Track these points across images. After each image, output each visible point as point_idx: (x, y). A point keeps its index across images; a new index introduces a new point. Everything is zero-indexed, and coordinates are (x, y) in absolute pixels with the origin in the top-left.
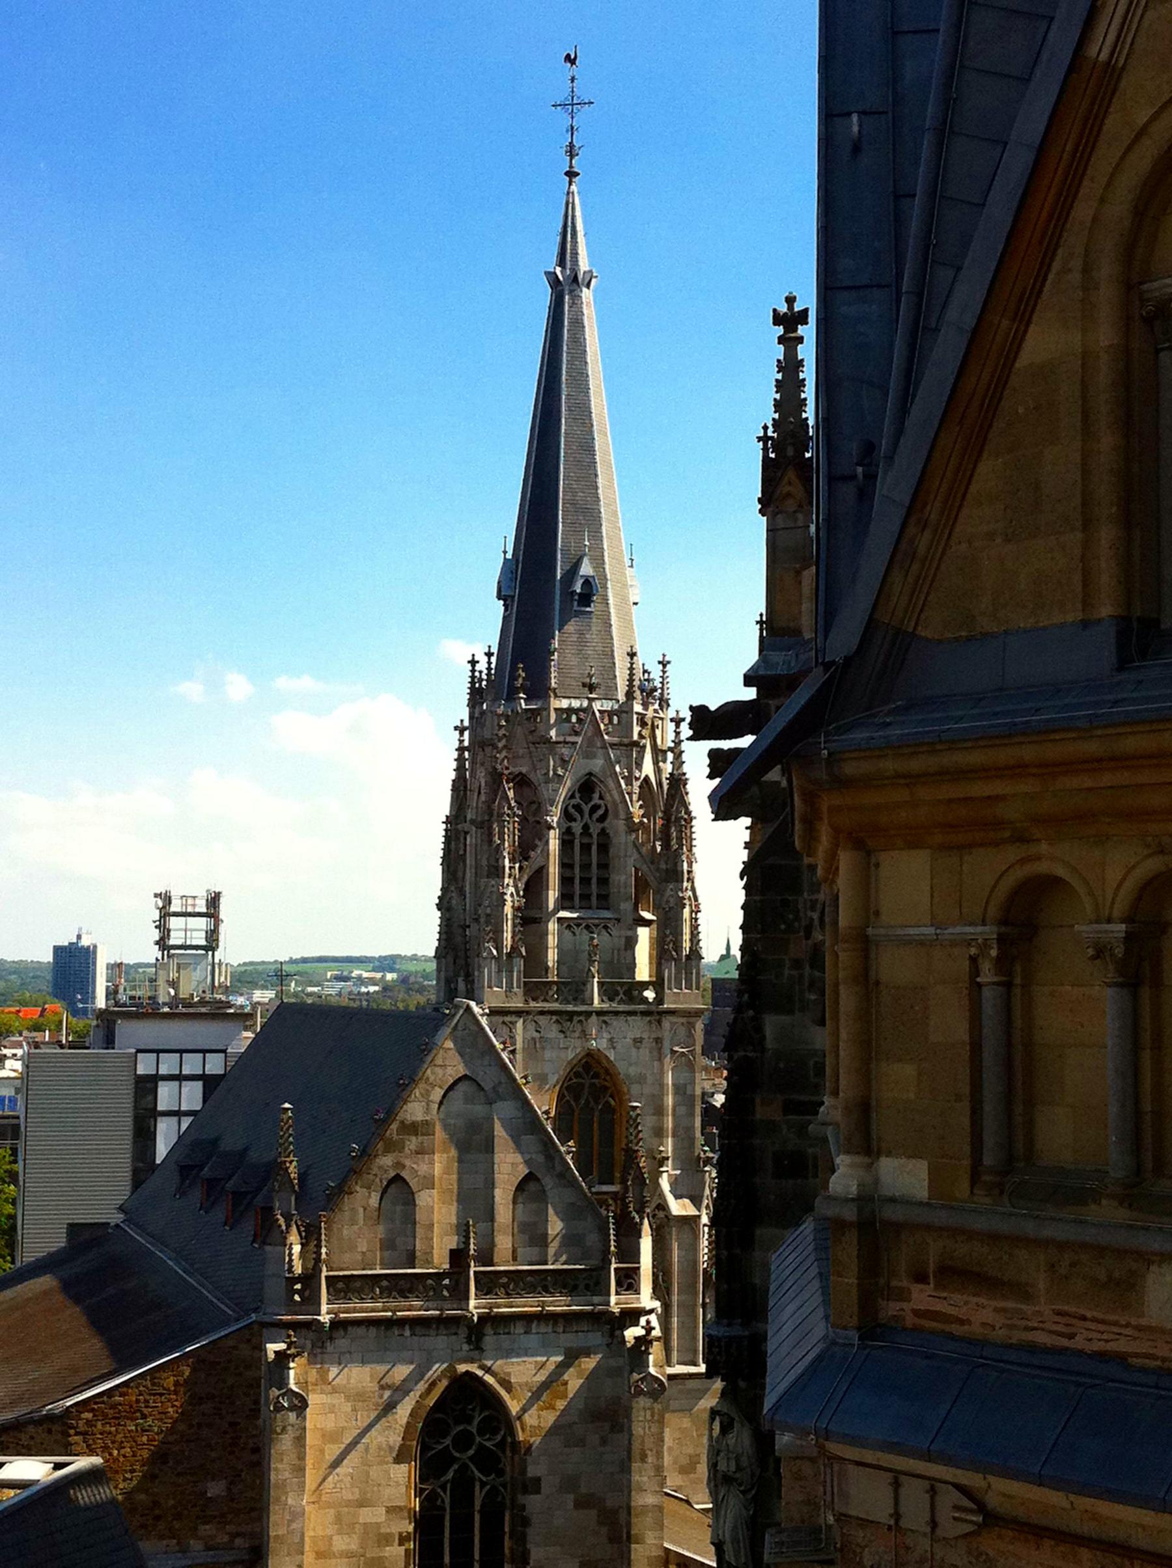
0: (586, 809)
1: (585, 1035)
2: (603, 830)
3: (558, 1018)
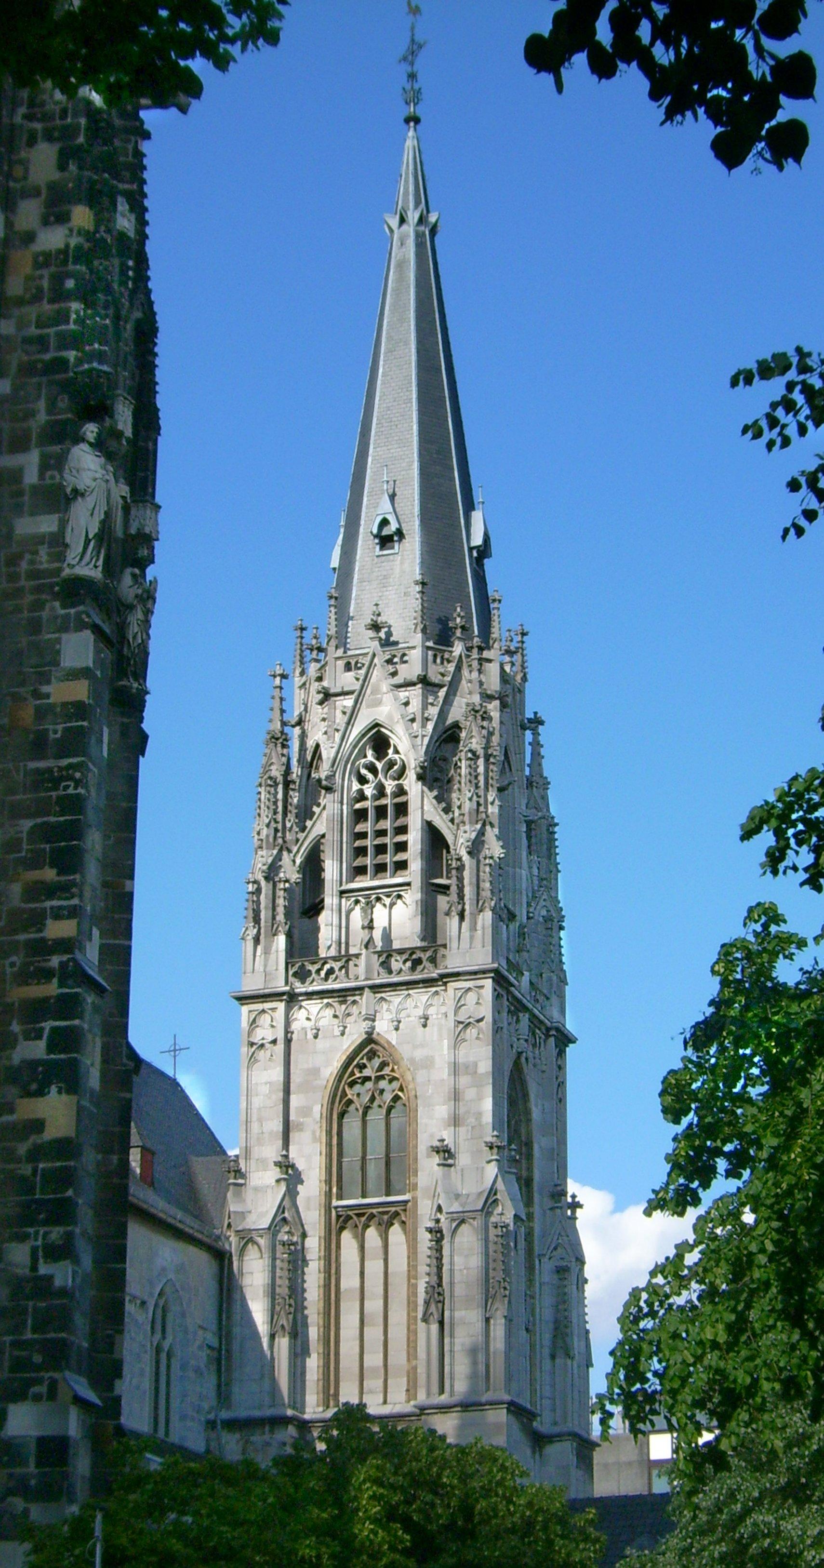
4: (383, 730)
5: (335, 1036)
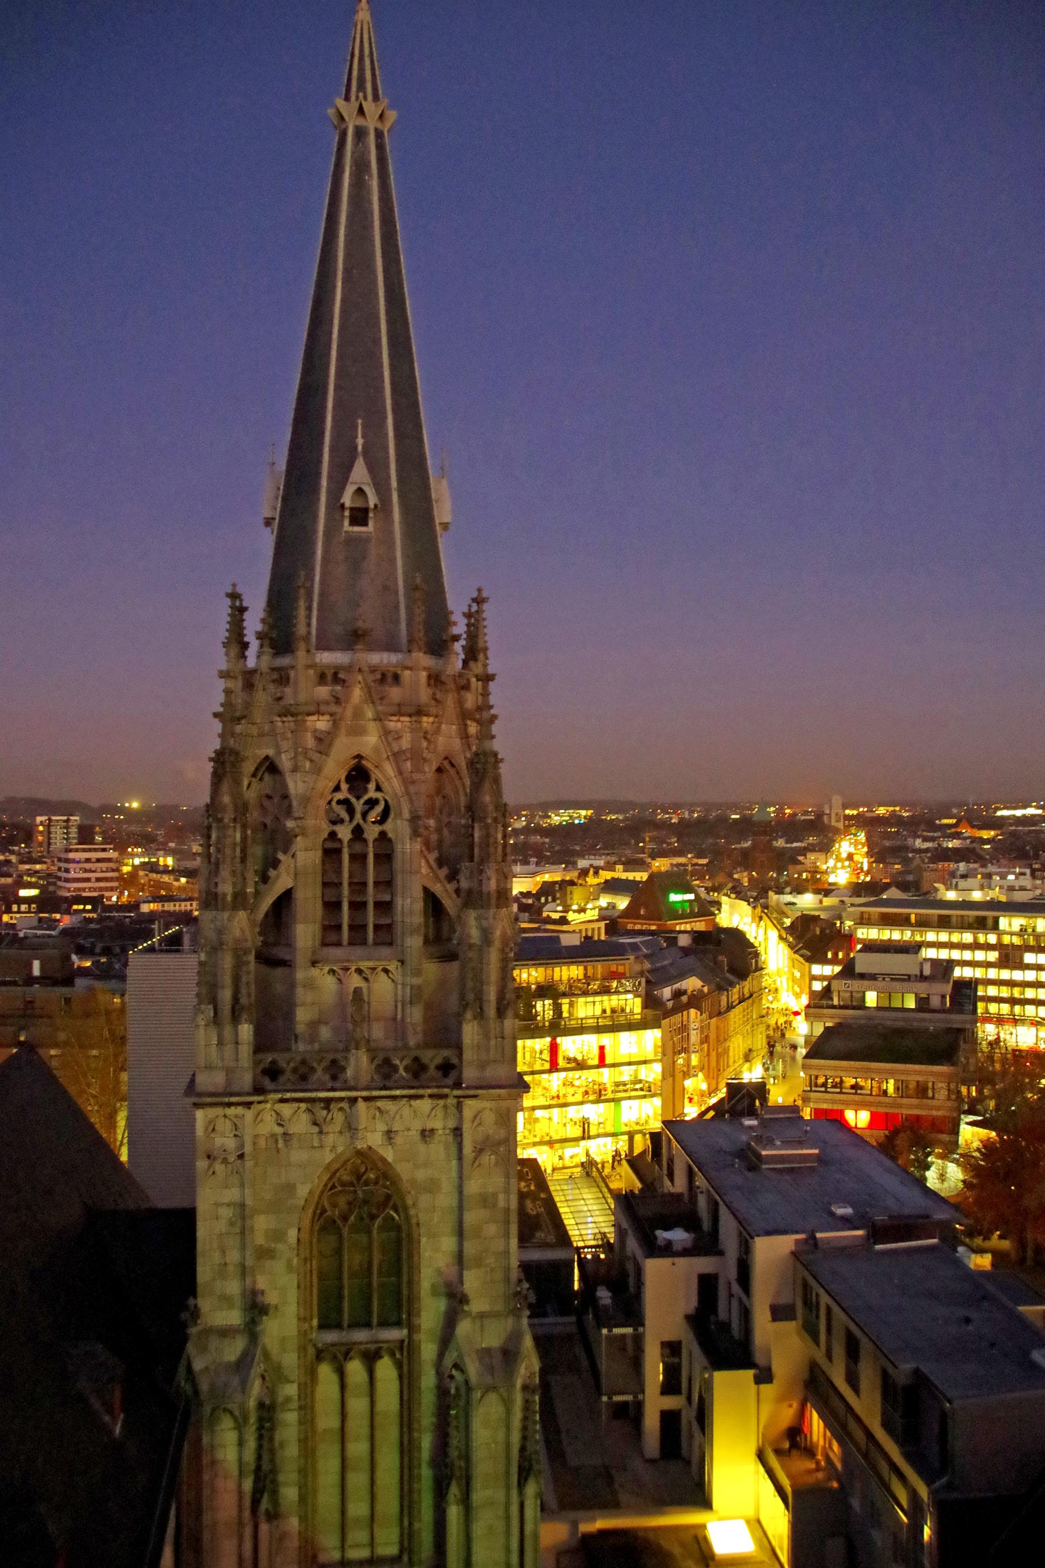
0: (359, 806)
1: (351, 1128)
2: (383, 834)
3: (309, 1105)
4: (364, 762)
5: (313, 1147)
